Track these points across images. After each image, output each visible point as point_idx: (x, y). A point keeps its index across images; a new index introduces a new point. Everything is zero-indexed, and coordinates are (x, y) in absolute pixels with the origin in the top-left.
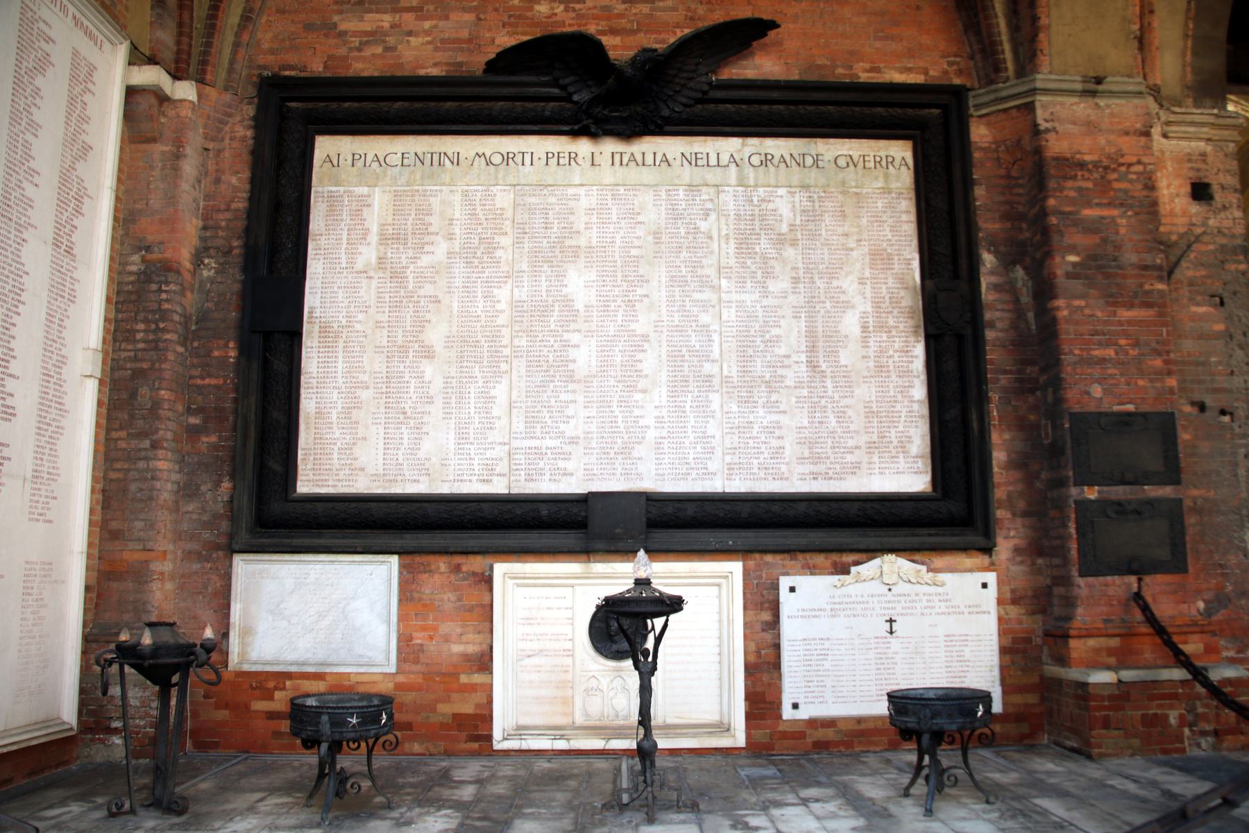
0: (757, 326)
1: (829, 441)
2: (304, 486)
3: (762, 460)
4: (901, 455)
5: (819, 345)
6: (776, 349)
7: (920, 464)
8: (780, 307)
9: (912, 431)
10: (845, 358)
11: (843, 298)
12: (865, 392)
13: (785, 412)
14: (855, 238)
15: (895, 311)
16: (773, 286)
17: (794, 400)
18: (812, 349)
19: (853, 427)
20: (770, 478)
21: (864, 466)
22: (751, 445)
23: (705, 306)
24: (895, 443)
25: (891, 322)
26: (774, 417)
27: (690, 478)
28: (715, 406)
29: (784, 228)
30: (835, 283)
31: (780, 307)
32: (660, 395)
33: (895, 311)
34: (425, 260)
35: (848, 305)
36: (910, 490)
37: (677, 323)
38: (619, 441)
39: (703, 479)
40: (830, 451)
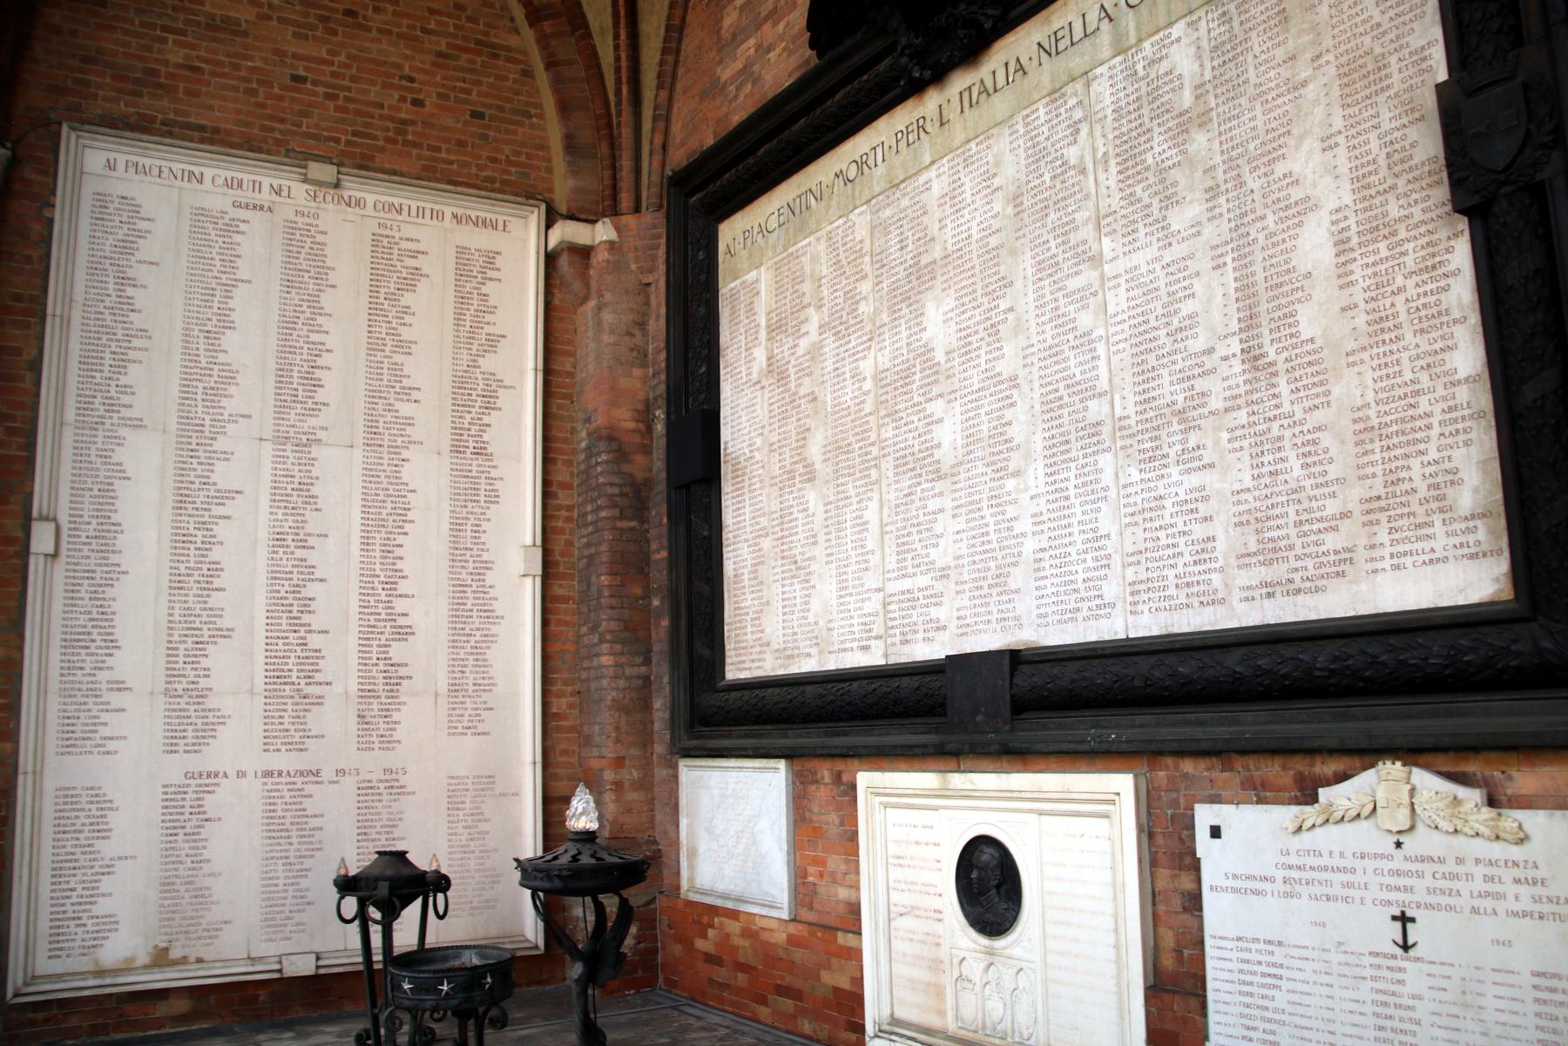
0: (1159, 305)
1: (1291, 510)
2: (733, 673)
3: (1180, 570)
4: (1437, 519)
5: (1262, 306)
6: (1190, 342)
7: (1481, 535)
8: (1191, 256)
9: (1459, 454)
10: (1308, 326)
11: (1296, 194)
12: (1353, 387)
13: (1212, 466)
14: (1308, 56)
15: (1401, 182)
16: (1179, 219)
17: (1225, 436)
18: (1249, 322)
19: (1334, 472)
20: (1195, 601)
21: (1361, 554)
22: (1164, 542)
23: (1082, 297)
24: (1423, 492)
25: (1394, 211)
26: (1195, 480)
27: (1080, 616)
28: (1107, 478)
29: (1187, 98)
30: (1280, 168)
31: (1191, 256)
32: (1036, 477)
33: (1401, 182)
34: (804, 344)
35: (1307, 206)
36: (1461, 601)
37: (1050, 342)
38: (992, 564)
39: (1097, 617)
40: (1293, 532)
